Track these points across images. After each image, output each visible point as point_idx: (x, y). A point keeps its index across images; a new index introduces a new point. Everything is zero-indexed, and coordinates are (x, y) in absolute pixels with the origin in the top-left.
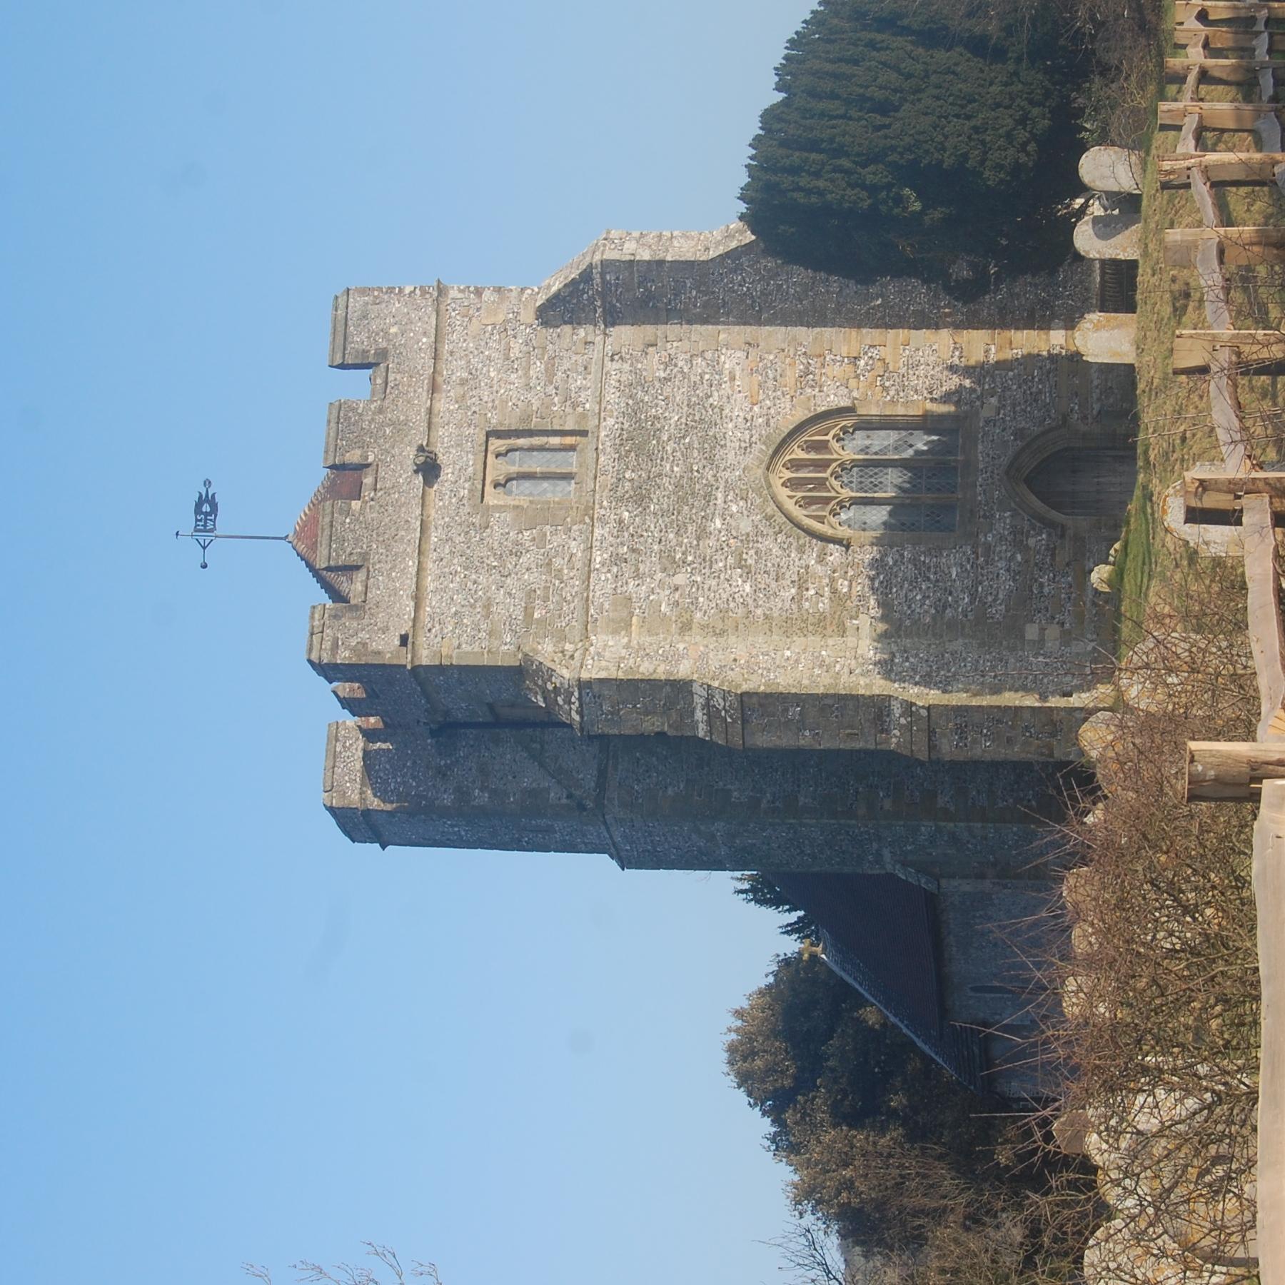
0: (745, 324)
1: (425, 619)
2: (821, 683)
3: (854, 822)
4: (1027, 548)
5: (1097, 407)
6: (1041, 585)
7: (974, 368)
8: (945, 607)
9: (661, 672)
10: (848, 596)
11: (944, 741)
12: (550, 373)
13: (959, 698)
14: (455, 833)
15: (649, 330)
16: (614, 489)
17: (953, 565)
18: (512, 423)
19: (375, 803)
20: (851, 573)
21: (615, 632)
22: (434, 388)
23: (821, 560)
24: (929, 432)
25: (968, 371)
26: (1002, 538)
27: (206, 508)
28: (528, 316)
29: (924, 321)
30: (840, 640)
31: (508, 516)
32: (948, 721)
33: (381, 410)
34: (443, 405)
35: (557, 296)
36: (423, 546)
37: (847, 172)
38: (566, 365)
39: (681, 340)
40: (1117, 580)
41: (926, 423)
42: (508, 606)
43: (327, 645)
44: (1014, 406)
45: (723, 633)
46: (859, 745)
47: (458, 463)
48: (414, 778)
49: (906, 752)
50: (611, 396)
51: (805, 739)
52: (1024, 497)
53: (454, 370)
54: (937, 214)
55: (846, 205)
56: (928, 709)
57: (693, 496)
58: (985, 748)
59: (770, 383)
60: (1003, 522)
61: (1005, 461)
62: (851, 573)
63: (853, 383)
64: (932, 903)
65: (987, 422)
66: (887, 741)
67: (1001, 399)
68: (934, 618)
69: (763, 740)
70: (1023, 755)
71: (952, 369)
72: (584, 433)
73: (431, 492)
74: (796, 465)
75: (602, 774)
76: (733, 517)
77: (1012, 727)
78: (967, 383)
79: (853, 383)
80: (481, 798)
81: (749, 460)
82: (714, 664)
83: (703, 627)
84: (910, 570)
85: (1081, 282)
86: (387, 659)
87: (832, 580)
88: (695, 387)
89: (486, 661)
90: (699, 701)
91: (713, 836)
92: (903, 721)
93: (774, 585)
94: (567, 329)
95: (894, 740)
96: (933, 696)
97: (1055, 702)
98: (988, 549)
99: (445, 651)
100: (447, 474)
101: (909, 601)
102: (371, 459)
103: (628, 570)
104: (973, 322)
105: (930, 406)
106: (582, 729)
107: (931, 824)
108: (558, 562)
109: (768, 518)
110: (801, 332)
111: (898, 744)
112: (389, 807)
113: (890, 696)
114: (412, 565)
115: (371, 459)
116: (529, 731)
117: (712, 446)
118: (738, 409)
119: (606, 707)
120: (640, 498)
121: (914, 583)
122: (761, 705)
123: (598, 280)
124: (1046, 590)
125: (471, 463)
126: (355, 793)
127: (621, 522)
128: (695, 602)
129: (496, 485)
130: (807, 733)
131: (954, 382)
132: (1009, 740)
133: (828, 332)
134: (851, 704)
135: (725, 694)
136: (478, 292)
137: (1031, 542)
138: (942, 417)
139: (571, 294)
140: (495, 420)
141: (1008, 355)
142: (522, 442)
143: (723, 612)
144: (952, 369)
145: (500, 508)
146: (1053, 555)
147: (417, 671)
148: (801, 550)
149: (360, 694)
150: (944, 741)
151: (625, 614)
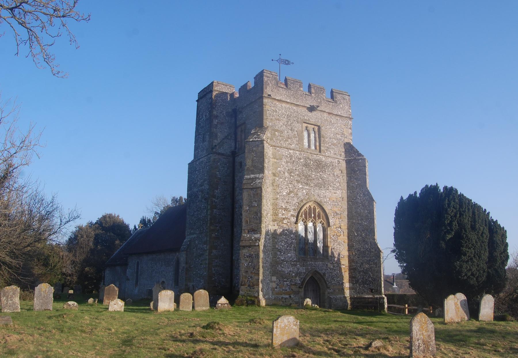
0: (348, 198)
1: (275, 102)
2: (264, 213)
3: (208, 225)
4: (296, 277)
5: (332, 297)
6: (286, 281)
7: (339, 261)
8: (280, 252)
9: (266, 165)
10: (283, 223)
11: (247, 251)
12: (334, 144)
13: (261, 255)
14: (202, 117)
15: (345, 172)
16: (308, 158)
17: (291, 254)
18: (322, 133)
19: (214, 94)
20: (289, 224)
21: (273, 154)
22: (329, 113)
23: (292, 215)
24: (323, 247)
25: (339, 259)
26: (298, 269)
27: (287, 62)
28: (346, 141)
29: (350, 247)
30: (271, 220)
31: (300, 129)
32: (254, 252)
33: (323, 99)
34: (325, 115)
35: (353, 147)
36: (293, 105)
37: (455, 216)
38: (336, 149)
39: (343, 180)
40: (306, 308)
41: (326, 247)
42: (280, 125)
43: (268, 75)
44: (331, 273)
45: (273, 185)
46: (244, 224)
47: (313, 117)
48: (221, 105)
49: (242, 239)
50: (330, 160)
51: (246, 208)
52: (308, 276)
53: (334, 119)
54: (443, 245)
55: (446, 215)
56: (259, 246)
57: (307, 180)
58: (244, 264)
59: (334, 204)
60: (303, 270)
61: (318, 270)
62: (289, 224)
63: (335, 227)
64: (176, 249)
65: (327, 265)
66: (245, 233)
67: (333, 269)
68: (277, 248)
69: (245, 194)
70: (241, 276)
71: (339, 255)
72: (320, 151)
73: (305, 109)
74: (315, 209)
75: (223, 154)
76: (303, 191)
77: (252, 273)
78: (336, 259)
79: (335, 227)
80: (215, 122)
81: (316, 197)
82: (267, 181)
83: (274, 179)
84: (290, 242)
85: (365, 292)
86: (265, 90)
87: (287, 218)
88: (333, 183)
89: (265, 117)
90: (257, 176)
91: (202, 186)
92: (253, 238)
93: (285, 201)
94: (344, 150)
95: (246, 235)
96: (262, 247)
97: (261, 286)
98: (296, 265)
99: (267, 106)
100: (310, 114)
101: (281, 241)
102: (313, 95)
103: (288, 160)
104: (351, 261)
105: (330, 248)
106: (247, 142)
107: (208, 248)
108: (290, 140)
109: (302, 201)
110: (346, 213)
111: (244, 236)
112: (213, 97)
113: (261, 234)
114: (288, 101)
115: (313, 95)
116: (233, 136)
117: (319, 186)
118: (328, 194)
119: (254, 149)
120: (306, 165)
121: (286, 242)
122: (257, 194)
123: (360, 157)
124: (285, 283)
125: (312, 121)
126: (217, 89)
127: (301, 159)
128: (280, 178)
129: (306, 127)
130: (248, 208)
131: (336, 256)
132: (247, 272)
133: (346, 220)
134: (258, 221)
135: (261, 183)
136: (350, 128)
137: (298, 278)
138: (327, 252)
139: (354, 151)
140: (323, 128)
141: (343, 271)
142: (317, 135)
143: (278, 186)
144: (339, 255)
145: (302, 127)
146: (294, 285)
147: (262, 97)
148: (294, 210)
149: (248, 88)
150: (247, 251)
151: (277, 158)
